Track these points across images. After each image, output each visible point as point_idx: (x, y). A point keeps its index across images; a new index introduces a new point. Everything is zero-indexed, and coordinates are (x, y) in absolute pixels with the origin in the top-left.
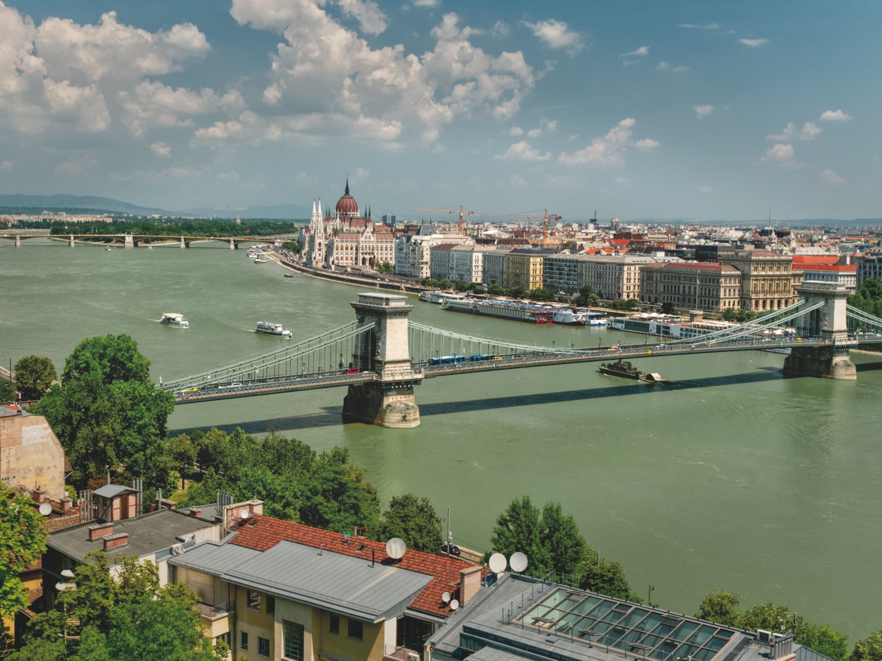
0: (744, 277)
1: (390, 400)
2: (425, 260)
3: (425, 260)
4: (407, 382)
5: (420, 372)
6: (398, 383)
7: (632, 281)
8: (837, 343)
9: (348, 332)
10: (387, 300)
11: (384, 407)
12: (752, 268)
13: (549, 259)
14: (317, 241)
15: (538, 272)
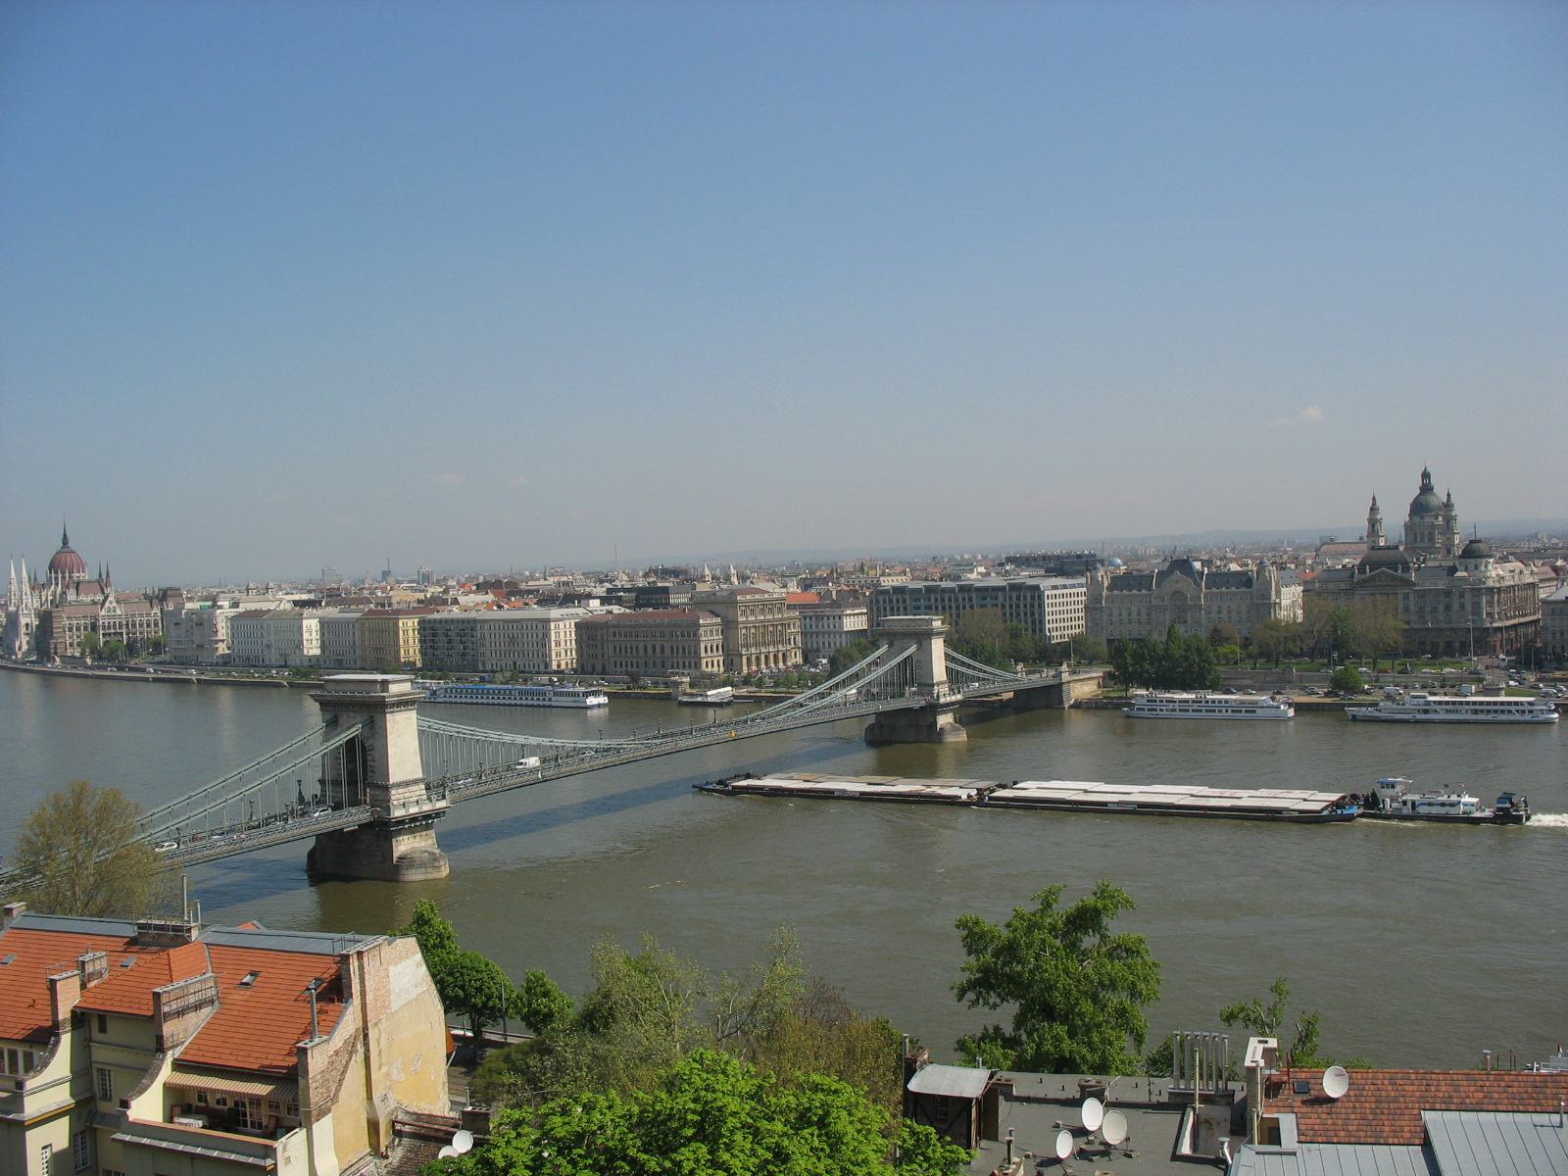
0: (728, 626)
1: (403, 845)
2: (220, 636)
3: (220, 636)
4: (427, 816)
5: (444, 797)
6: (414, 819)
7: (563, 643)
8: (942, 700)
9: (307, 745)
10: (385, 683)
11: (395, 860)
12: (739, 613)
13: (430, 621)
14: (23, 621)
15: (411, 642)
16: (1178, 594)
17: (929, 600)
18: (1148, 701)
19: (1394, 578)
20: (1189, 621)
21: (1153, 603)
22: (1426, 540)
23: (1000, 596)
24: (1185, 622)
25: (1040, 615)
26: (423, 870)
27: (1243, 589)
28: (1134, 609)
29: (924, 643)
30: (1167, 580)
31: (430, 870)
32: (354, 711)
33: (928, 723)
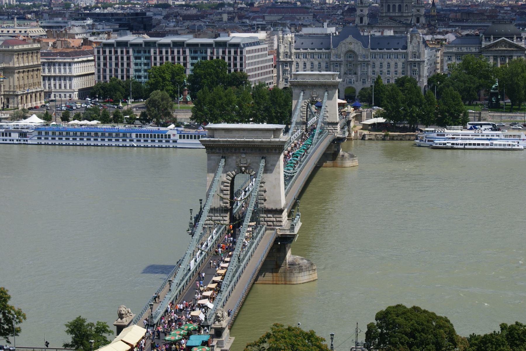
16: (351, 53)
17: (149, 52)
18: (438, 135)
19: (511, 45)
20: (359, 73)
21: (332, 59)
22: (397, 11)
23: (209, 51)
24: (355, 74)
25: (241, 65)
26: (307, 273)
27: (401, 51)
28: (316, 63)
29: (330, 92)
30: (344, 41)
31: (311, 272)
32: (245, 153)
33: (332, 152)
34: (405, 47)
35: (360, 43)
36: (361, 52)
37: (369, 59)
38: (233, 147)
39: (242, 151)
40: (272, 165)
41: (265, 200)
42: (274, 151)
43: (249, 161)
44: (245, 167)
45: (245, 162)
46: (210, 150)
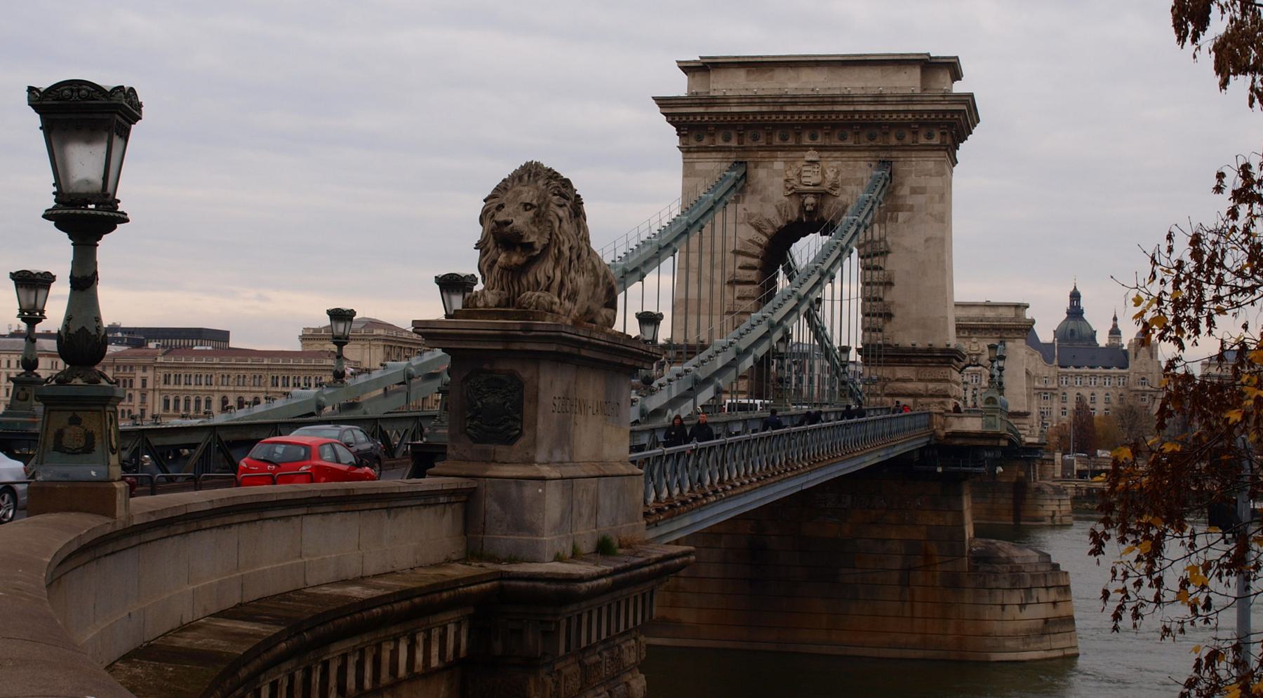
27: (1114, 370)
32: (819, 149)
33: (1014, 480)
34: (1125, 366)
35: (1038, 355)
36: (1040, 372)
37: (1055, 385)
38: (776, 126)
39: (806, 140)
40: (914, 191)
41: (889, 316)
42: (923, 140)
43: (830, 175)
44: (816, 194)
45: (816, 179)
46: (693, 143)
